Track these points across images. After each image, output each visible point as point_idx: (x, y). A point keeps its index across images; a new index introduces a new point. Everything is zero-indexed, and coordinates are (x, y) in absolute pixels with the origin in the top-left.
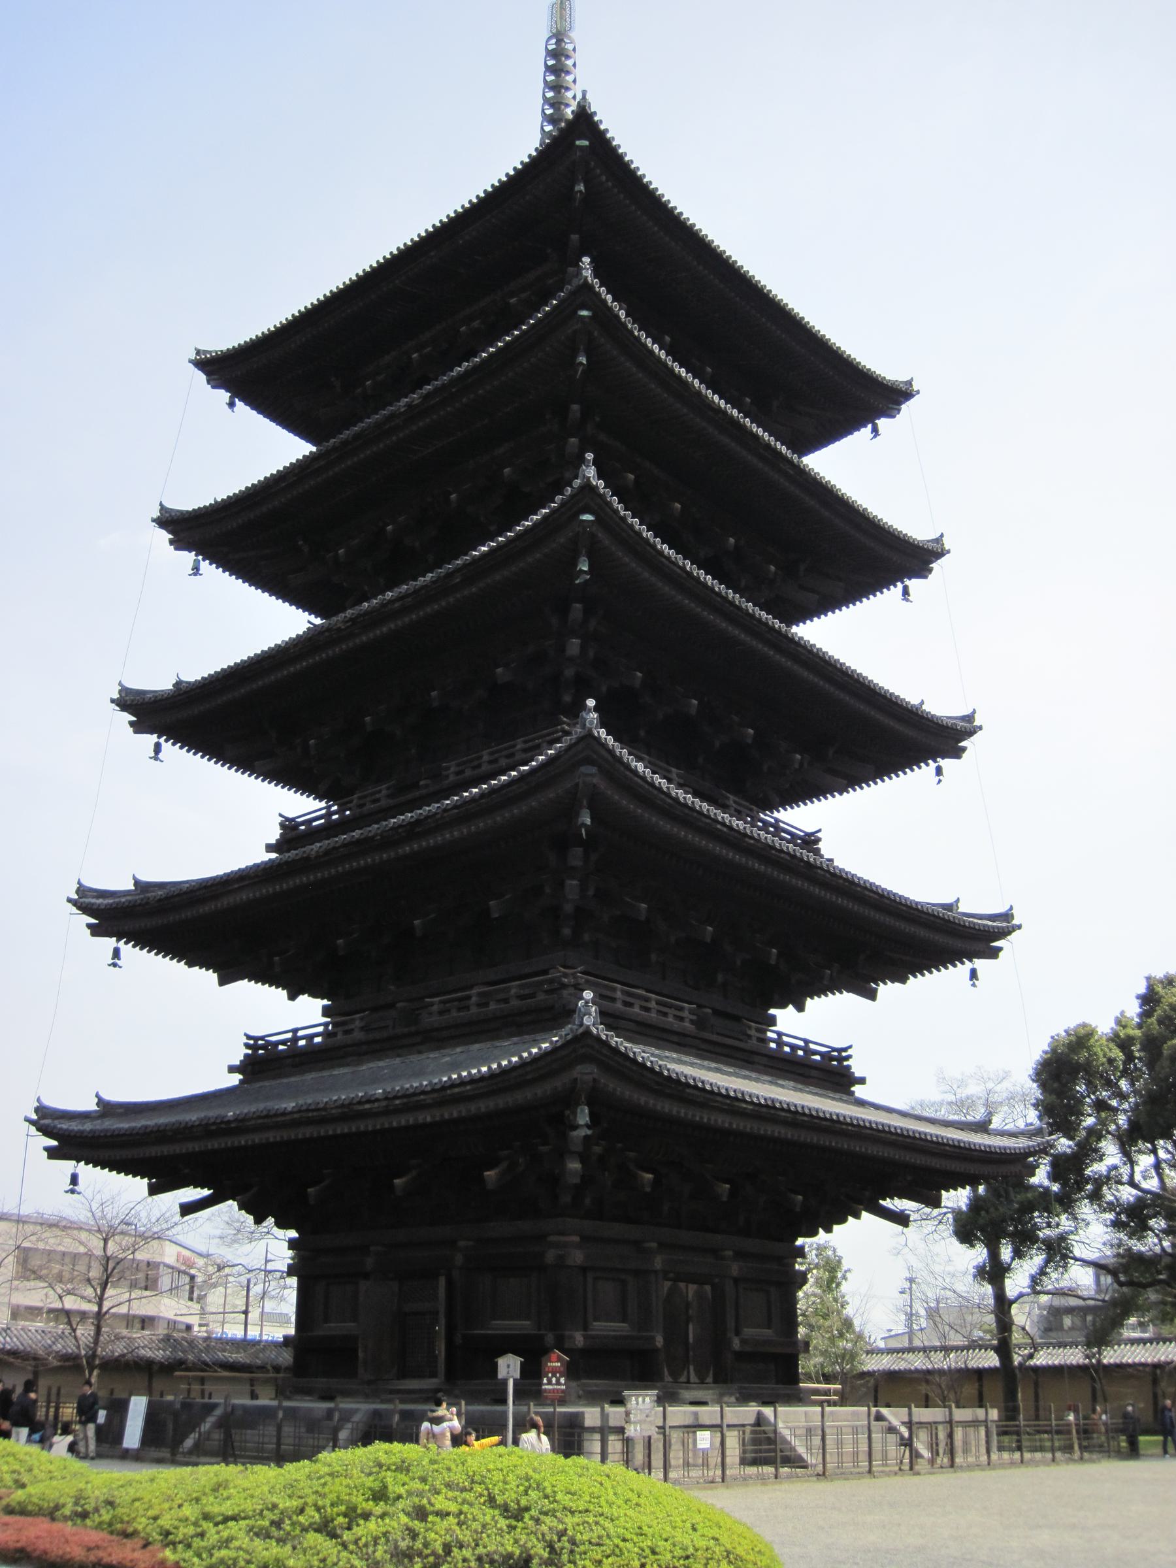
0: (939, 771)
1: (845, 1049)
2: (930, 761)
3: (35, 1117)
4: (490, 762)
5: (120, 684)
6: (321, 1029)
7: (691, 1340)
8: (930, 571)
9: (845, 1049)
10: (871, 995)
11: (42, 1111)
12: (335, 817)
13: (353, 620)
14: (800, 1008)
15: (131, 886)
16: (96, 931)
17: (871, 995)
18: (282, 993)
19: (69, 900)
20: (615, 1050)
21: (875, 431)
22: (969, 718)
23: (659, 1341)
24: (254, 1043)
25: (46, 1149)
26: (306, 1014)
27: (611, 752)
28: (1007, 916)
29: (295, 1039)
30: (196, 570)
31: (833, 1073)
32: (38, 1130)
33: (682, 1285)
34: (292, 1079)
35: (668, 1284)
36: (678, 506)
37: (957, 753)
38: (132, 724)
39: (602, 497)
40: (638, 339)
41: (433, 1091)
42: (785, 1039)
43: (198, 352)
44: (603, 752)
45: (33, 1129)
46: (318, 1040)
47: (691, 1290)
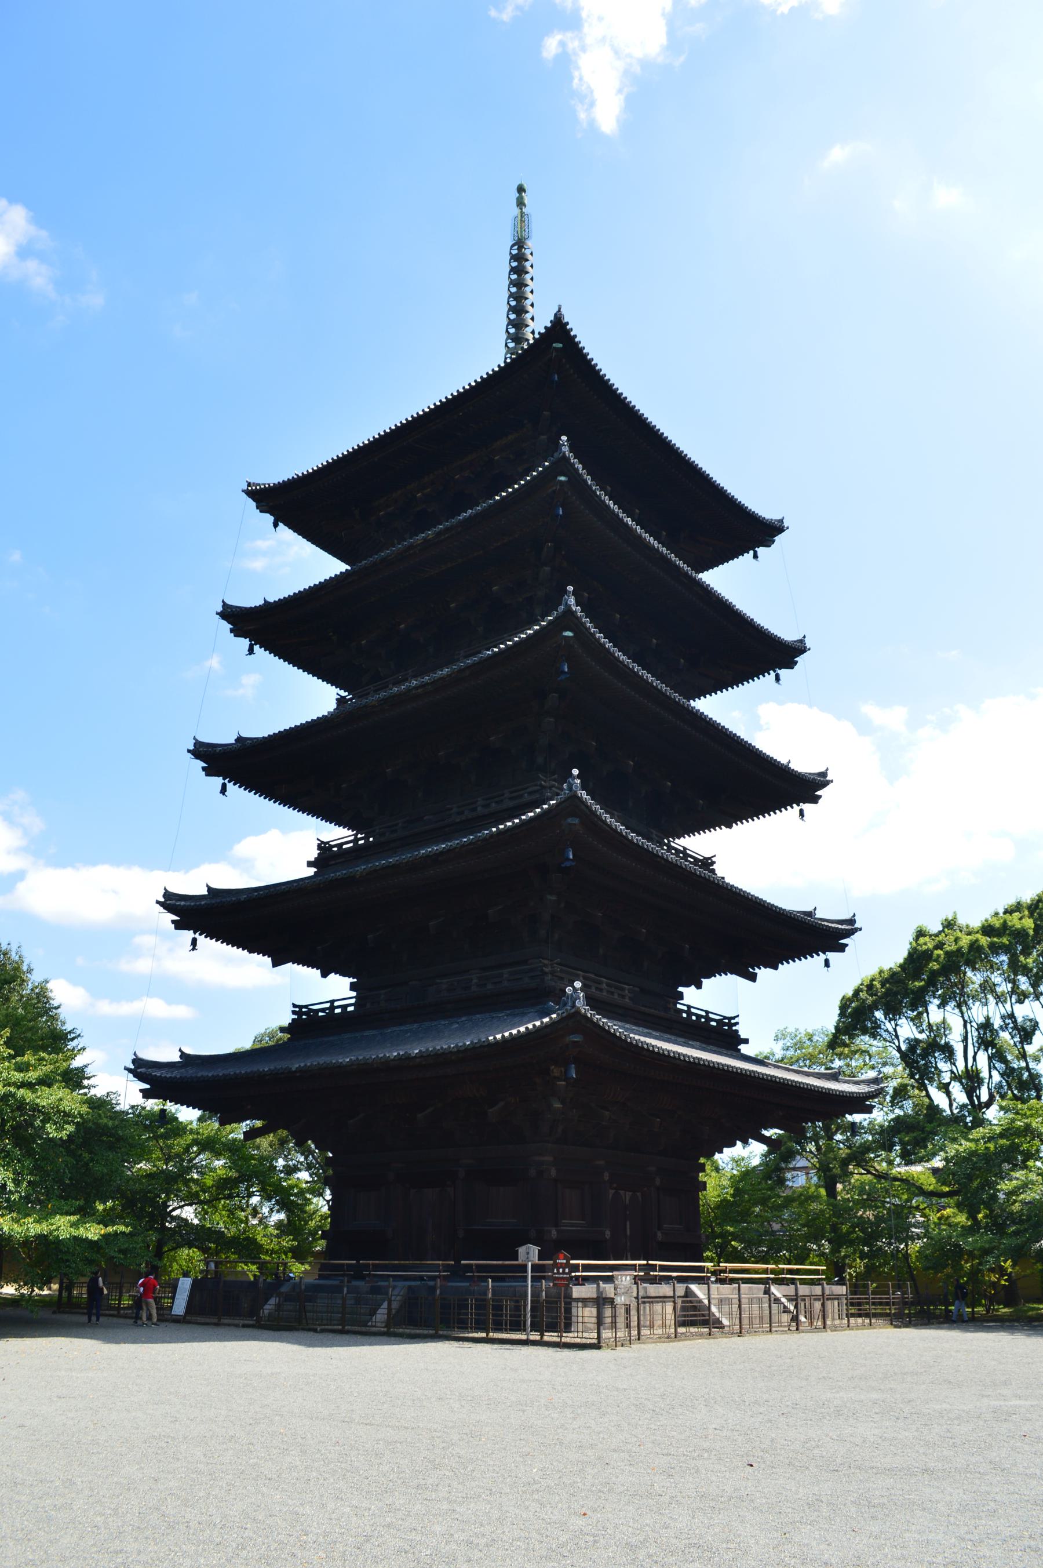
0: (802, 813)
1: (734, 1018)
2: (794, 805)
3: (132, 1067)
4: (483, 806)
5: (194, 738)
6: (353, 1001)
7: (628, 1233)
8: (796, 662)
9: (734, 1018)
10: (753, 978)
11: (137, 1061)
12: (360, 842)
13: (385, 700)
14: (699, 986)
15: (204, 892)
16: (178, 925)
17: (753, 978)
18: (316, 973)
19: (158, 902)
20: (596, 1025)
21: (755, 556)
22: (824, 774)
23: (608, 1234)
24: (299, 1010)
25: (141, 1091)
26: (337, 989)
27: (589, 808)
28: (851, 921)
29: (332, 1008)
30: (251, 651)
31: (724, 1035)
32: (135, 1076)
33: (622, 1192)
34: (331, 1038)
35: (612, 1192)
36: (618, 616)
37: (815, 800)
38: (204, 769)
39: (578, 619)
40: (599, 497)
41: (459, 1051)
42: (693, 1010)
43: (249, 484)
44: (583, 807)
45: (131, 1076)
46: (350, 1009)
47: (627, 1196)
